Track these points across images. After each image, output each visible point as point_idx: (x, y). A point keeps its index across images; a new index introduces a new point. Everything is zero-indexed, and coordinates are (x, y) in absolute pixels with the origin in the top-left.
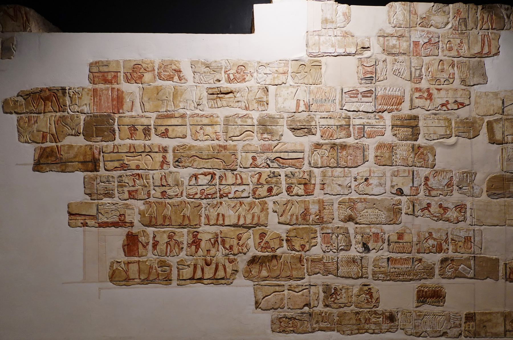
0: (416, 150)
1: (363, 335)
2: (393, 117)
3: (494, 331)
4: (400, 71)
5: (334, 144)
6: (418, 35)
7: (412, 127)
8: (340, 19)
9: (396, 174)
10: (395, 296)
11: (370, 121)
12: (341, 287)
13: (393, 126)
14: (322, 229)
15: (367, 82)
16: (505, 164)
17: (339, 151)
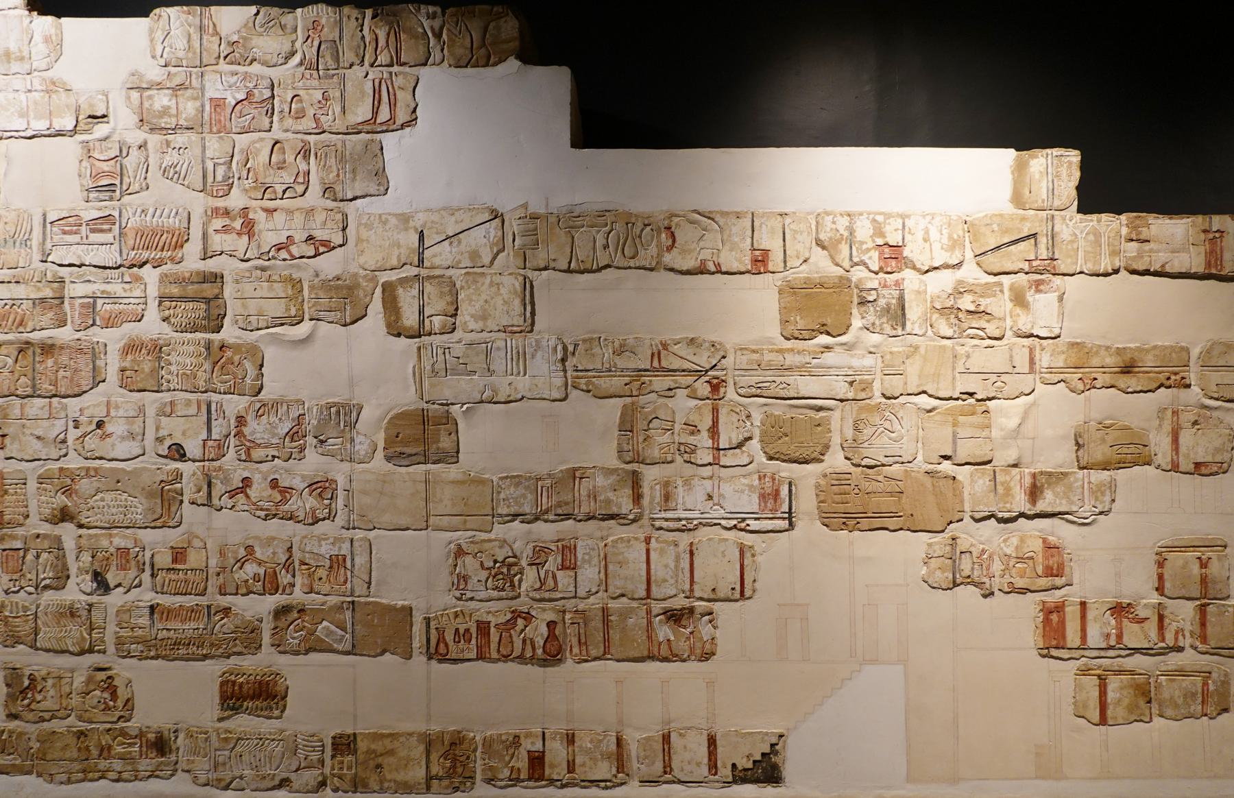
0: (217, 355)
1: (96, 784)
2: (163, 279)
3: (400, 777)
4: (178, 169)
5: (27, 343)
6: (221, 85)
7: (208, 301)
8: (39, 49)
9: (168, 410)
10: (173, 695)
11: (109, 288)
12: (44, 673)
13: (162, 299)
15: (102, 196)
17: (37, 359)
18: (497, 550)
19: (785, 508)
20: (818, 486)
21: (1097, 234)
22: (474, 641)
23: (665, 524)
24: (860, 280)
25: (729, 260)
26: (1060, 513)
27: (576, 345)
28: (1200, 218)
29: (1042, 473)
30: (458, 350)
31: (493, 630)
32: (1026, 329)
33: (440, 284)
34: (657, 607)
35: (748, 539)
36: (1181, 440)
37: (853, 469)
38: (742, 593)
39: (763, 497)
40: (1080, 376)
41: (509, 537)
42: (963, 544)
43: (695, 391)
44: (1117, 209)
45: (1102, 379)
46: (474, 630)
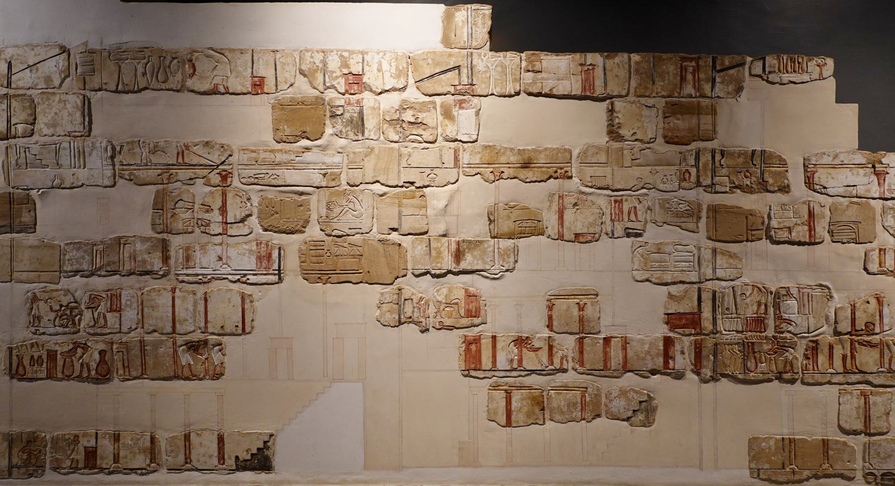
16: (12, 174)
18: (63, 298)
19: (276, 266)
20: (300, 250)
21: (504, 67)
22: (45, 365)
23: (186, 278)
24: (331, 99)
25: (235, 84)
26: (477, 271)
27: (122, 147)
28: (577, 56)
29: (464, 241)
30: (35, 149)
31: (59, 356)
32: (452, 135)
33: (22, 100)
34: (180, 340)
35: (248, 290)
36: (565, 217)
37: (326, 238)
38: (244, 330)
39: (259, 259)
40: (491, 170)
41: (72, 288)
42: (406, 294)
43: (209, 180)
44: (519, 48)
45: (508, 172)
46: (45, 357)
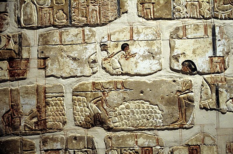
14: (44, 142)
